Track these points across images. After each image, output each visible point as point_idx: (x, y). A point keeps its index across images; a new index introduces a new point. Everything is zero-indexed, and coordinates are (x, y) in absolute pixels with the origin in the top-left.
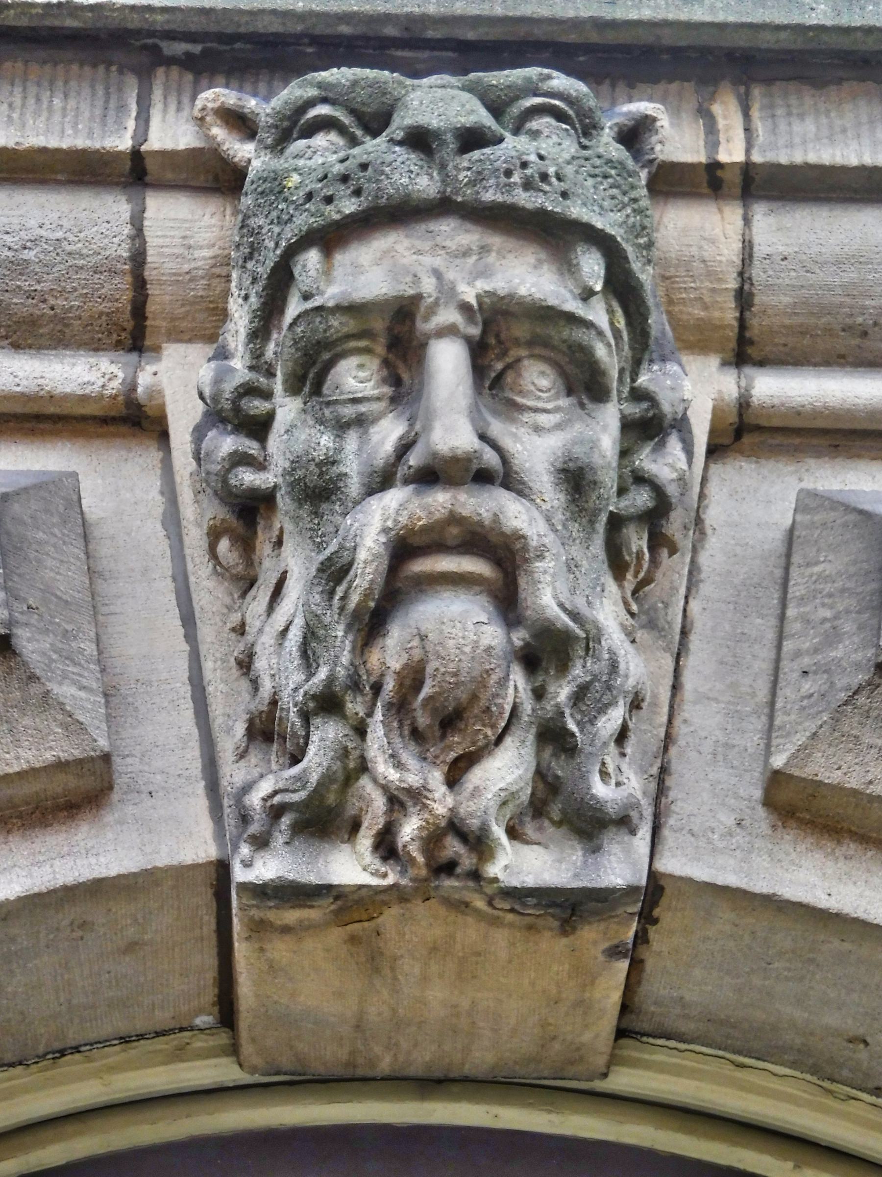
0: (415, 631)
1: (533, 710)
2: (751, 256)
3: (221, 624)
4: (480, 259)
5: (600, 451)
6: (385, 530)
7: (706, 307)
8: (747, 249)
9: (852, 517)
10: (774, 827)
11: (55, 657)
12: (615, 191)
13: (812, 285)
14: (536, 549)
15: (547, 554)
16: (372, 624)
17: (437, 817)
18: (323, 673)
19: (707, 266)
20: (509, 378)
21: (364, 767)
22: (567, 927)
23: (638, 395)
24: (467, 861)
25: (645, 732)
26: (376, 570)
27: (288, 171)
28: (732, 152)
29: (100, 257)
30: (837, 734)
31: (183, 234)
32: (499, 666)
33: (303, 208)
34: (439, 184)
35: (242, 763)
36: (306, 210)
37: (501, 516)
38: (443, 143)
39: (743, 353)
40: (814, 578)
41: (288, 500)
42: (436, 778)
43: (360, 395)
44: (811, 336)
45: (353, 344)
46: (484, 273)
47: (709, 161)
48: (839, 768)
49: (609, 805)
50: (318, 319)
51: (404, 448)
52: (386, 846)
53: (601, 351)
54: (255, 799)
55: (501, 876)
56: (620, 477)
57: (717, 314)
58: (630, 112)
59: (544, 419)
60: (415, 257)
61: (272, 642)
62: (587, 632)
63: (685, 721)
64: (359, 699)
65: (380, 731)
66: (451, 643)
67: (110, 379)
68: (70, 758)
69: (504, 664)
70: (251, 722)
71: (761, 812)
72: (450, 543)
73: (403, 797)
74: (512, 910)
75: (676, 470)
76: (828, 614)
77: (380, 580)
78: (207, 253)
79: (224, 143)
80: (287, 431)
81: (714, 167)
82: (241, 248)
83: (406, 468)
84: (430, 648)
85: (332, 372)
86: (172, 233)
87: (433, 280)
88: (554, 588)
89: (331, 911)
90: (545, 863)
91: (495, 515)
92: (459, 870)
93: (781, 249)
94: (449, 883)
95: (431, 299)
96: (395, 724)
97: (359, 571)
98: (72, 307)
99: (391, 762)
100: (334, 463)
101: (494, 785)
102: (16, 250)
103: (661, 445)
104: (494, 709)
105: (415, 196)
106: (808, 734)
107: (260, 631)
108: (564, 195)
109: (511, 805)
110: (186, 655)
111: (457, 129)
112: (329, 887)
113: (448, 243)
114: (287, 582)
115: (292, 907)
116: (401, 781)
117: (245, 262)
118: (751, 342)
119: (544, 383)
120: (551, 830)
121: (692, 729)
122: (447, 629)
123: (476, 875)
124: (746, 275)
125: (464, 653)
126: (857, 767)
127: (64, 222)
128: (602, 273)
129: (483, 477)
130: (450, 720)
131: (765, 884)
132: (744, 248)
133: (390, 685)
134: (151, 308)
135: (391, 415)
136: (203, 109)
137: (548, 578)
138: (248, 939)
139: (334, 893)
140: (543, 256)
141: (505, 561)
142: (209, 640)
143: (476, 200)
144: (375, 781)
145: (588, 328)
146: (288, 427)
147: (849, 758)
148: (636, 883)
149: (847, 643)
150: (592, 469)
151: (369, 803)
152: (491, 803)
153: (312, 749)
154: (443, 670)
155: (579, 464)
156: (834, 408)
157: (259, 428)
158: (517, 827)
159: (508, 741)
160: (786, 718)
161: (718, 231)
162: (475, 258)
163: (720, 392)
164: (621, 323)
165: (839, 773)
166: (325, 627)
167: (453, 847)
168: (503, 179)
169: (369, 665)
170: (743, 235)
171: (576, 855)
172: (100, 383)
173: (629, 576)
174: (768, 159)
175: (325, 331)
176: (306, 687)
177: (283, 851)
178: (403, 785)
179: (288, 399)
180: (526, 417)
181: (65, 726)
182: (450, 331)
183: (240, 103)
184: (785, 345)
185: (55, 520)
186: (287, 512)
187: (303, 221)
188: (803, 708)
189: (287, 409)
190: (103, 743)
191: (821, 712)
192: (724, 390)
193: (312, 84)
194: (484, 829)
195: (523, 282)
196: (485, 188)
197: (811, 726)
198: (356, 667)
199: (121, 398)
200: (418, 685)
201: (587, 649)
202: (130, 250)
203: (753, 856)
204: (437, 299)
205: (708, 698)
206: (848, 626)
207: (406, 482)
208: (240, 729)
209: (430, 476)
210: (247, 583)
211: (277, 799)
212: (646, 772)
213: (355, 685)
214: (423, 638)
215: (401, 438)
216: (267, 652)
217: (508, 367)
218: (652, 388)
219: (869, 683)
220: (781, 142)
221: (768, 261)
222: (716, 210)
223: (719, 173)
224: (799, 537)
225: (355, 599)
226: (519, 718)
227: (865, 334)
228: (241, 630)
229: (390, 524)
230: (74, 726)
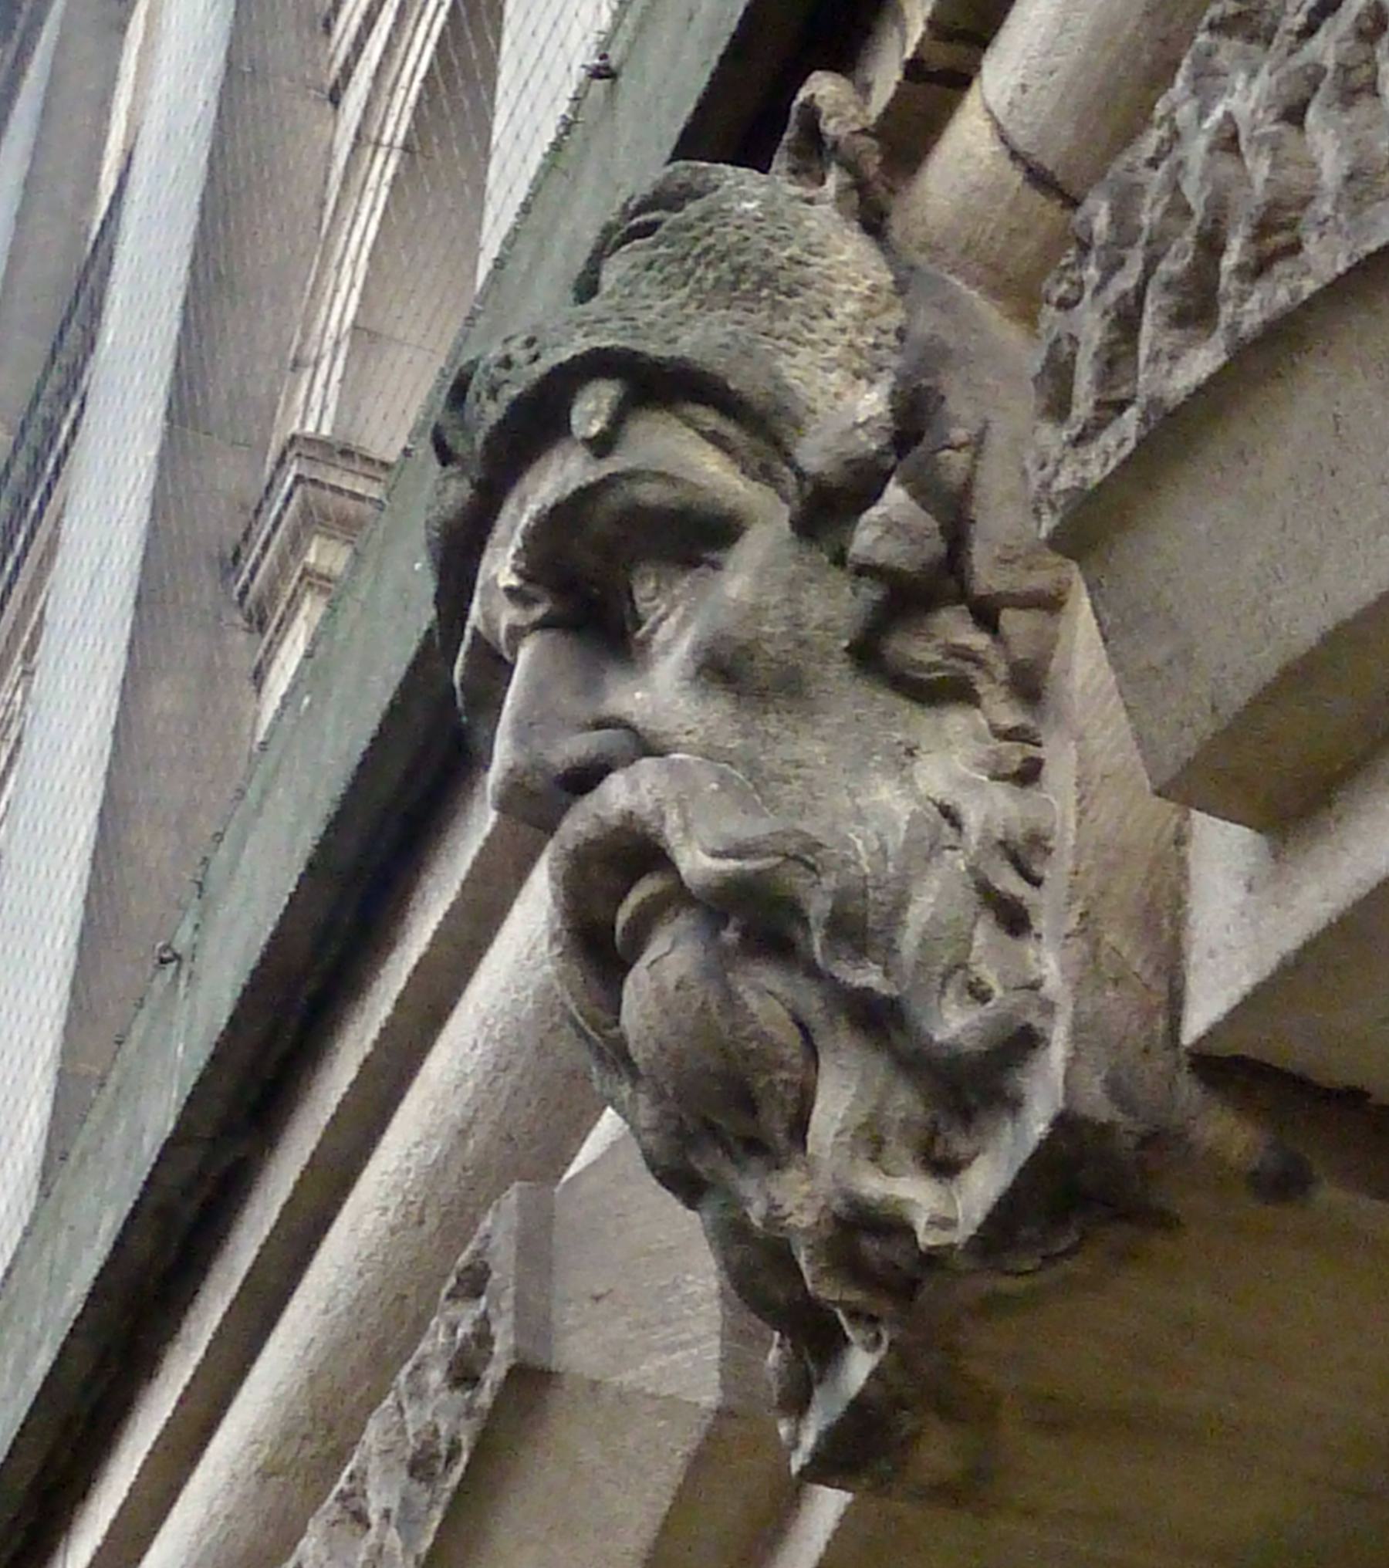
7: (1027, 233)
32: (707, 992)
49: (962, 1040)
105: (451, 516)
123: (933, 1259)
154: (650, 1056)
164: (711, 419)
181: (661, 1414)
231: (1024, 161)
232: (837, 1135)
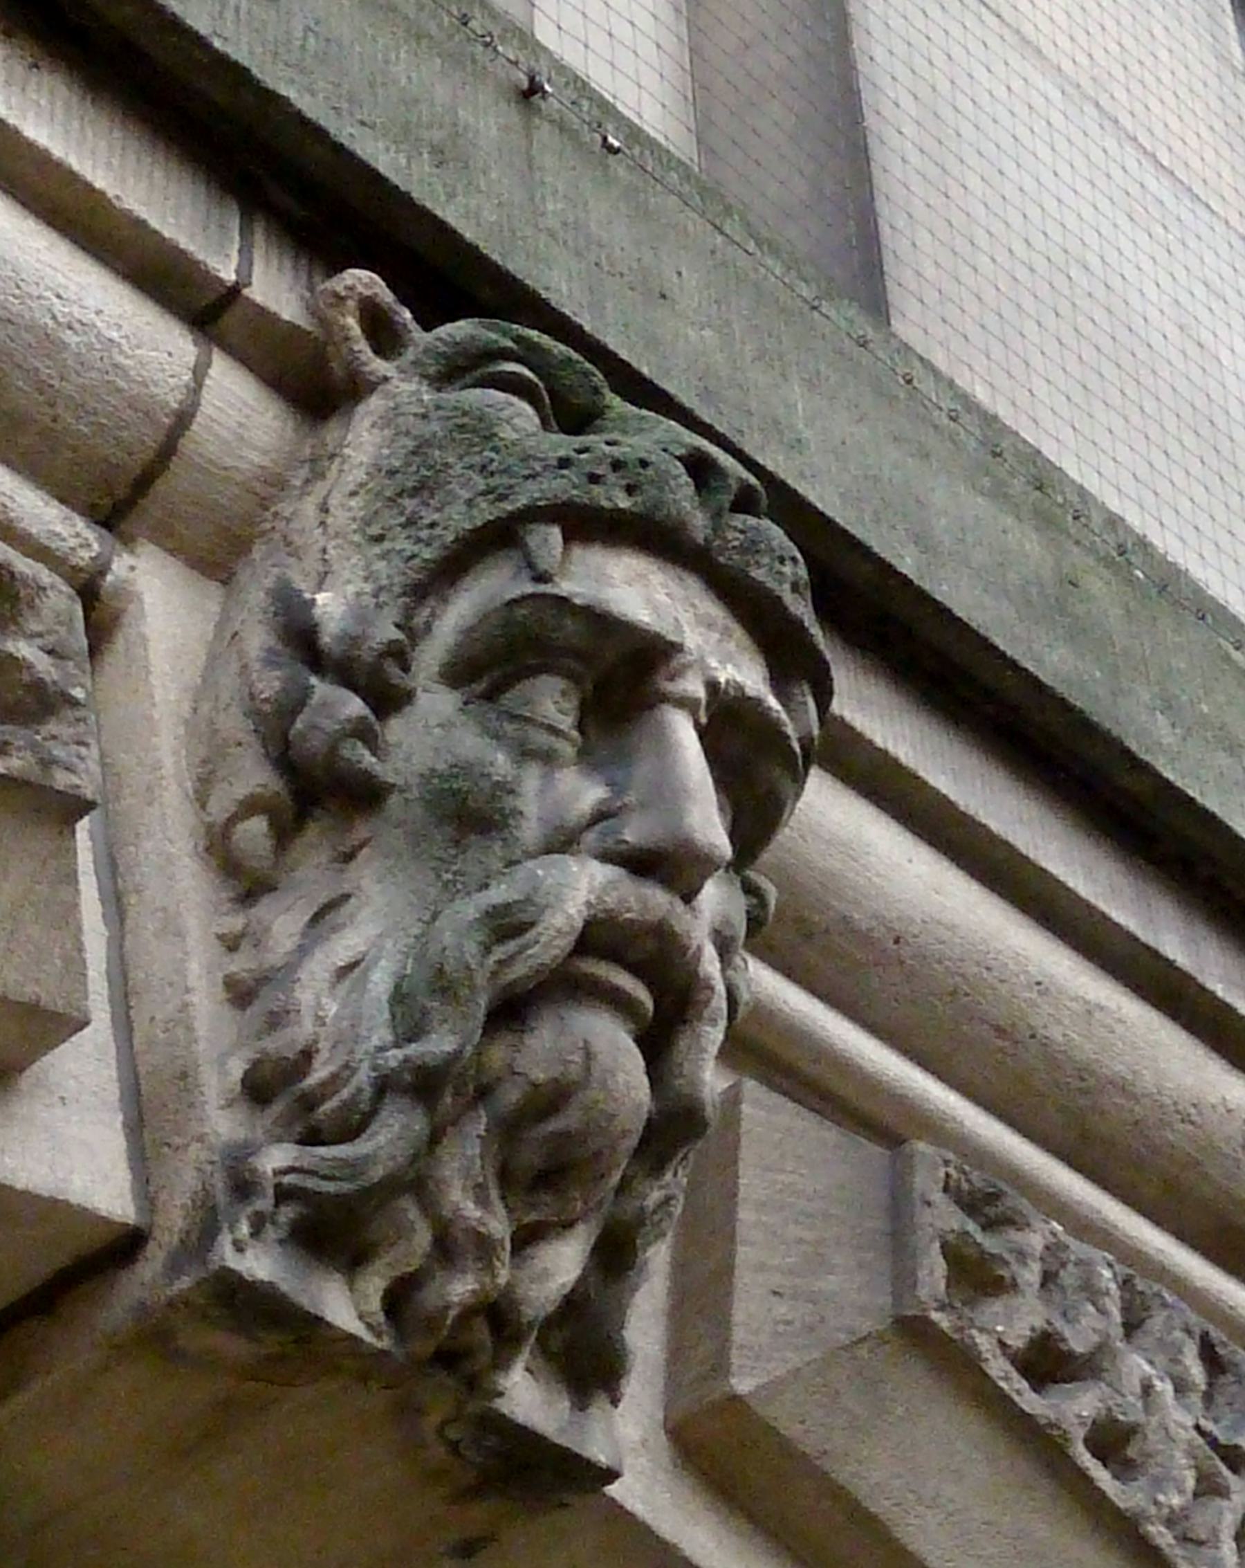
16: (511, 1011)
48: (802, 1422)
52: (398, 1299)
66: (621, 1078)
67: (81, 546)
78: (255, 457)
84: (596, 1073)
102: (59, 324)
116: (479, 1220)
133: (511, 1096)
134: (160, 486)
136: (351, 288)
166: (472, 988)
172: (73, 542)
178: (482, 1229)
181: (67, 960)
193: (505, 334)
196: (757, 562)
197: (795, 1359)
202: (181, 403)
211: (287, 1179)
214: (588, 1055)
225: (519, 970)
227: (809, 936)
229: (592, 898)
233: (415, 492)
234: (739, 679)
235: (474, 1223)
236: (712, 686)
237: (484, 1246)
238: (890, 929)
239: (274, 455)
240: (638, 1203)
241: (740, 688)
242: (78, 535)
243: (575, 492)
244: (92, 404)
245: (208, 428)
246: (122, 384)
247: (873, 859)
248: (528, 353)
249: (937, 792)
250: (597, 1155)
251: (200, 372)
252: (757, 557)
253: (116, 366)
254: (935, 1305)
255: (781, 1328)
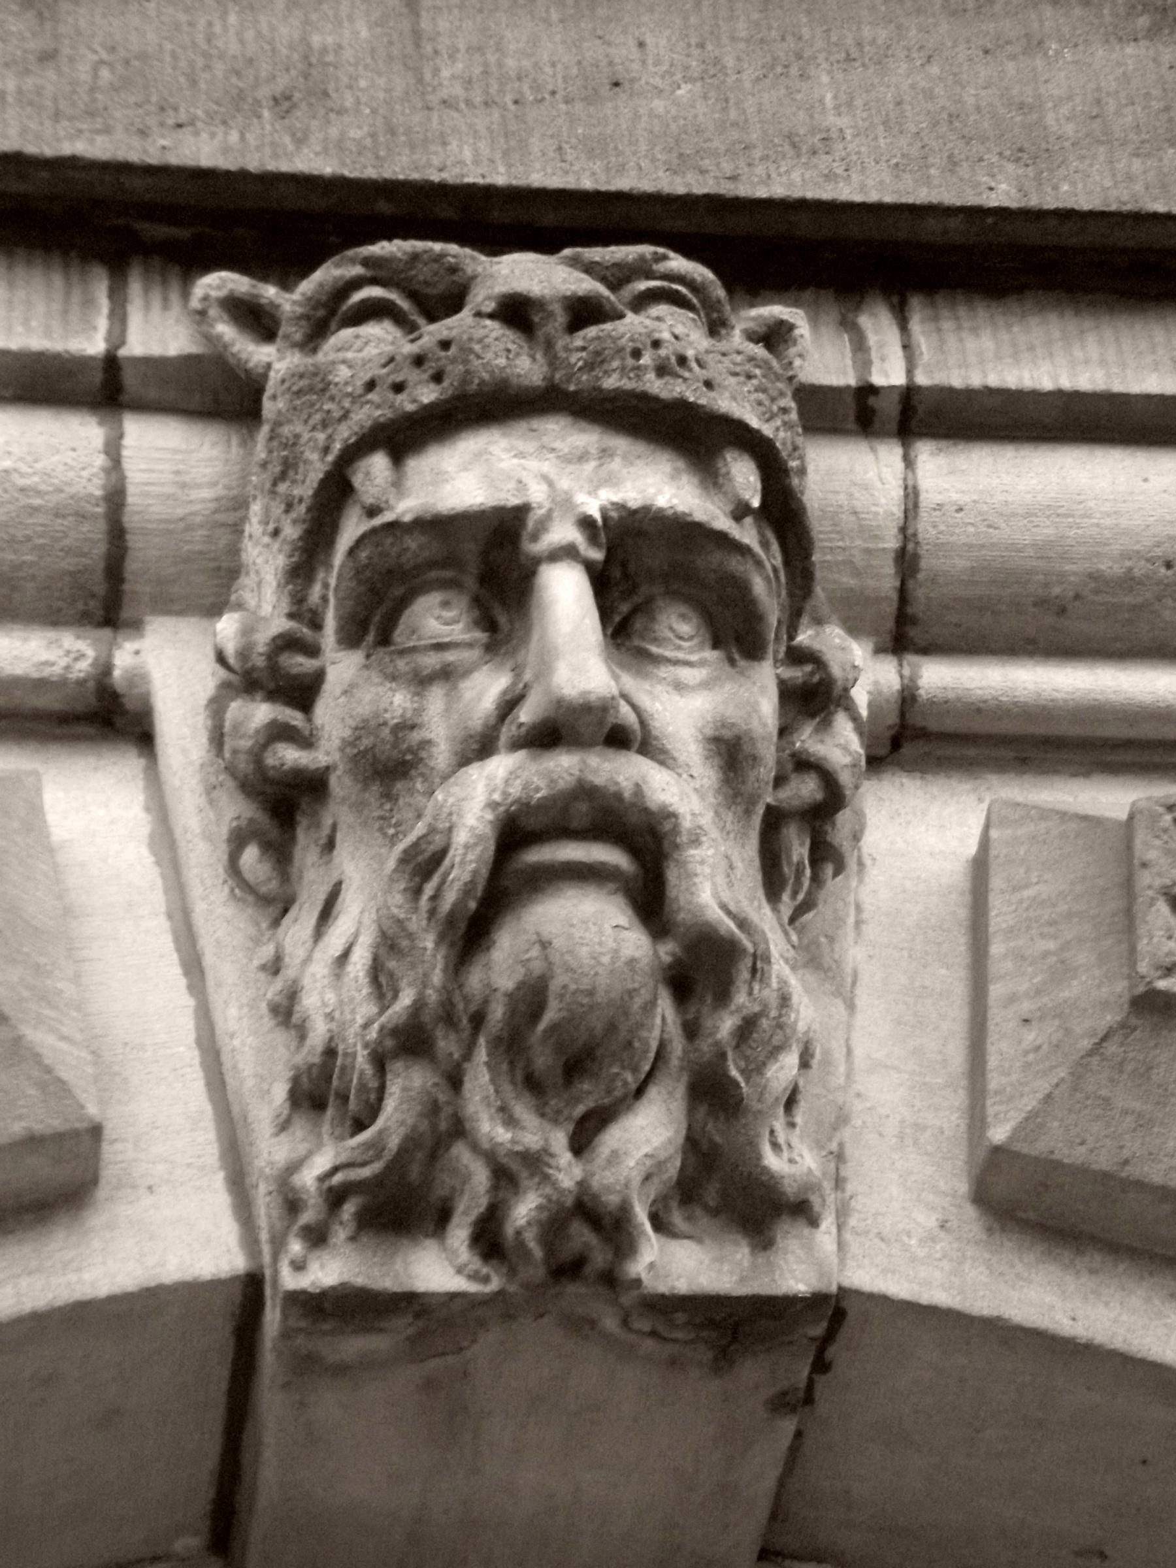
0: (534, 937)
1: (684, 1051)
2: (916, 505)
3: (244, 961)
4: (601, 465)
5: (760, 718)
6: (492, 805)
7: (857, 573)
8: (911, 496)
9: (1073, 826)
10: (990, 1230)
11: (26, 994)
12: (761, 396)
13: (993, 544)
14: (689, 831)
15: (704, 839)
16: (472, 932)
17: (562, 1192)
18: (406, 999)
19: (859, 519)
20: (638, 624)
21: (459, 1129)
22: (724, 1359)
23: (797, 656)
24: (600, 1258)
25: (818, 1096)
26: (480, 856)
27: (333, 363)
28: (889, 373)
29: (63, 495)
30: (1078, 1095)
31: (175, 468)
32: (645, 985)
33: (363, 399)
34: (545, 369)
35: (283, 1136)
36: (367, 402)
37: (644, 787)
38: (551, 315)
39: (903, 636)
40: (1025, 905)
41: (347, 781)
42: (559, 1140)
43: (447, 640)
44: (993, 612)
45: (433, 574)
46: (610, 481)
47: (860, 384)
48: (1082, 1143)
49: (786, 1182)
50: (389, 540)
51: (509, 705)
52: (489, 1240)
53: (759, 586)
54: (308, 1178)
55: (644, 1276)
56: (779, 762)
57: (871, 583)
58: (760, 316)
59: (688, 675)
60: (516, 461)
61: (326, 971)
62: (755, 944)
63: (858, 1095)
64: (453, 1036)
65: (485, 1077)
66: (584, 951)
67: (76, 659)
68: (48, 1131)
69: (652, 983)
70: (296, 1081)
71: (971, 1211)
72: (575, 824)
73: (514, 1166)
74: (653, 1334)
75: (850, 754)
76: (1051, 945)
77: (485, 872)
78: (206, 494)
79: (233, 345)
80: (345, 692)
81: (867, 391)
82: (270, 467)
83: (514, 728)
84: (556, 958)
85: (407, 612)
86: (161, 467)
87: (544, 487)
88: (714, 884)
89: (408, 1339)
90: (701, 1263)
91: (637, 785)
92: (588, 1270)
93: (955, 497)
94: (573, 1289)
95: (542, 511)
96: (505, 1067)
97: (458, 859)
98: (24, 562)
99: (497, 1119)
100: (413, 727)
101: (638, 1149)
103: (826, 724)
104: (637, 1044)
105: (515, 381)
106: (1040, 1096)
107: (307, 960)
108: (708, 384)
109: (656, 1180)
110: (190, 1012)
111: (566, 298)
112: (411, 1297)
113: (557, 444)
114: (340, 899)
115: (355, 1332)
116: (513, 1141)
117: (275, 484)
118: (914, 621)
119: (685, 628)
120: (704, 1221)
121: (868, 1105)
122: (577, 933)
123: (610, 1280)
124: (910, 531)
125: (599, 963)
126: (1108, 1142)
127: (15, 449)
128: (759, 486)
129: (618, 739)
130: (577, 1064)
131: (986, 1304)
132: (906, 496)
133: (497, 1012)
134: (132, 566)
135: (485, 668)
136: (206, 298)
137: (707, 870)
138: (286, 1386)
139: (416, 1307)
140: (681, 464)
141: (645, 855)
142: (230, 981)
143: (594, 389)
144: (475, 1148)
145: (743, 555)
146: (345, 687)
147: (1096, 1127)
148: (824, 1290)
149: (1084, 978)
150: (752, 739)
151: (466, 1178)
152: (634, 1173)
153: (390, 1105)
154: (573, 987)
155: (735, 731)
156: (1026, 704)
157: (302, 693)
158: (661, 1213)
159: (653, 1092)
160: (1004, 1080)
161: (871, 475)
162: (593, 464)
163: (876, 683)
165: (1083, 1149)
166: (411, 936)
167: (581, 1235)
168: (630, 362)
169: (466, 990)
170: (905, 479)
171: (741, 1253)
172: (63, 662)
173: (786, 897)
174: (936, 382)
175: (399, 556)
176: (383, 1019)
177: (348, 1249)
179: (341, 654)
180: (664, 671)
181: (42, 1086)
182: (567, 552)
183: (255, 291)
184: (958, 625)
185: (16, 825)
186: (344, 799)
187: (364, 416)
188: (1027, 1065)
189: (342, 667)
190: (92, 1110)
191: (1055, 1067)
192: (882, 681)
193: (353, 261)
194: (625, 1209)
195: (659, 492)
196: (606, 372)
197: (1043, 1086)
198: (448, 992)
199: (91, 684)
200: (536, 1013)
201: (754, 970)
202: (104, 487)
203: (967, 1266)
204: (550, 511)
205: (886, 1067)
206: (1083, 957)
207: (516, 745)
208: (280, 1092)
209: (548, 736)
210: (277, 905)
211: (338, 1178)
212: (823, 1148)
213: (448, 1017)
214: (545, 945)
215: (504, 693)
216: (318, 985)
217: (635, 610)
218: (816, 646)
219: (1123, 1025)
220: (951, 361)
221: (938, 513)
222: (868, 450)
223: (872, 401)
224: (997, 857)
225: (450, 898)
226: (666, 1063)
227: (1062, 611)
228: (274, 967)
229: (497, 797)
230: (54, 1087)
231: (906, 539)
232: (646, 1155)
233: (283, 476)
234: (616, 498)
235: (509, 1146)
236: (586, 523)
237: (535, 1161)
238: (1150, 560)
239: (225, 481)
240: (710, 1041)
241: (621, 507)
242: (68, 652)
243: (379, 412)
244: (20, 534)
245: (147, 495)
246: (37, 502)
247: (1092, 504)
248: (379, 272)
249: (1148, 398)
250: (612, 1028)
251: (113, 450)
252: (605, 366)
253: (22, 490)
254: (1159, 973)
255: (1031, 1057)
